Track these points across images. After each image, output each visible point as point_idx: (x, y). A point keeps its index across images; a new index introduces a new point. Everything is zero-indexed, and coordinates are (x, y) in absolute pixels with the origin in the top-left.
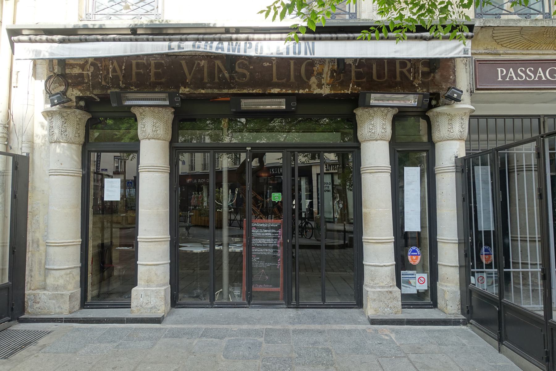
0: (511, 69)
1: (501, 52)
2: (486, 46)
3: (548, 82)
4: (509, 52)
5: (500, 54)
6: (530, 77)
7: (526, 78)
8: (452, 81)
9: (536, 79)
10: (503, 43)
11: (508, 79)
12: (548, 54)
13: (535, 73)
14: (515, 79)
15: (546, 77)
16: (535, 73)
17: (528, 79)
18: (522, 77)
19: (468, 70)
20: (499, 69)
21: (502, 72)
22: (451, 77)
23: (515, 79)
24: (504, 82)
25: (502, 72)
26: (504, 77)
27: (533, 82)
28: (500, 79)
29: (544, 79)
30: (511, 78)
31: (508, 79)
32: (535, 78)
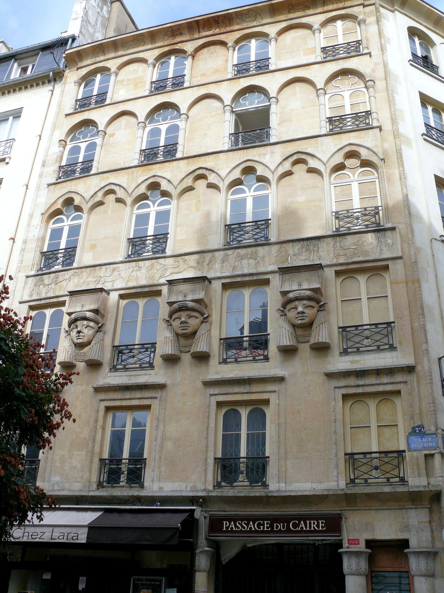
0: (232, 522)
1: (227, 510)
3: (256, 531)
6: (244, 528)
9: (248, 529)
11: (229, 529)
13: (247, 525)
14: (234, 529)
15: (254, 528)
16: (247, 525)
20: (225, 522)
21: (226, 524)
24: (227, 531)
25: (226, 524)
26: (227, 528)
27: (246, 532)
28: (224, 529)
29: (253, 529)
30: (232, 528)
31: (229, 529)
32: (247, 528)
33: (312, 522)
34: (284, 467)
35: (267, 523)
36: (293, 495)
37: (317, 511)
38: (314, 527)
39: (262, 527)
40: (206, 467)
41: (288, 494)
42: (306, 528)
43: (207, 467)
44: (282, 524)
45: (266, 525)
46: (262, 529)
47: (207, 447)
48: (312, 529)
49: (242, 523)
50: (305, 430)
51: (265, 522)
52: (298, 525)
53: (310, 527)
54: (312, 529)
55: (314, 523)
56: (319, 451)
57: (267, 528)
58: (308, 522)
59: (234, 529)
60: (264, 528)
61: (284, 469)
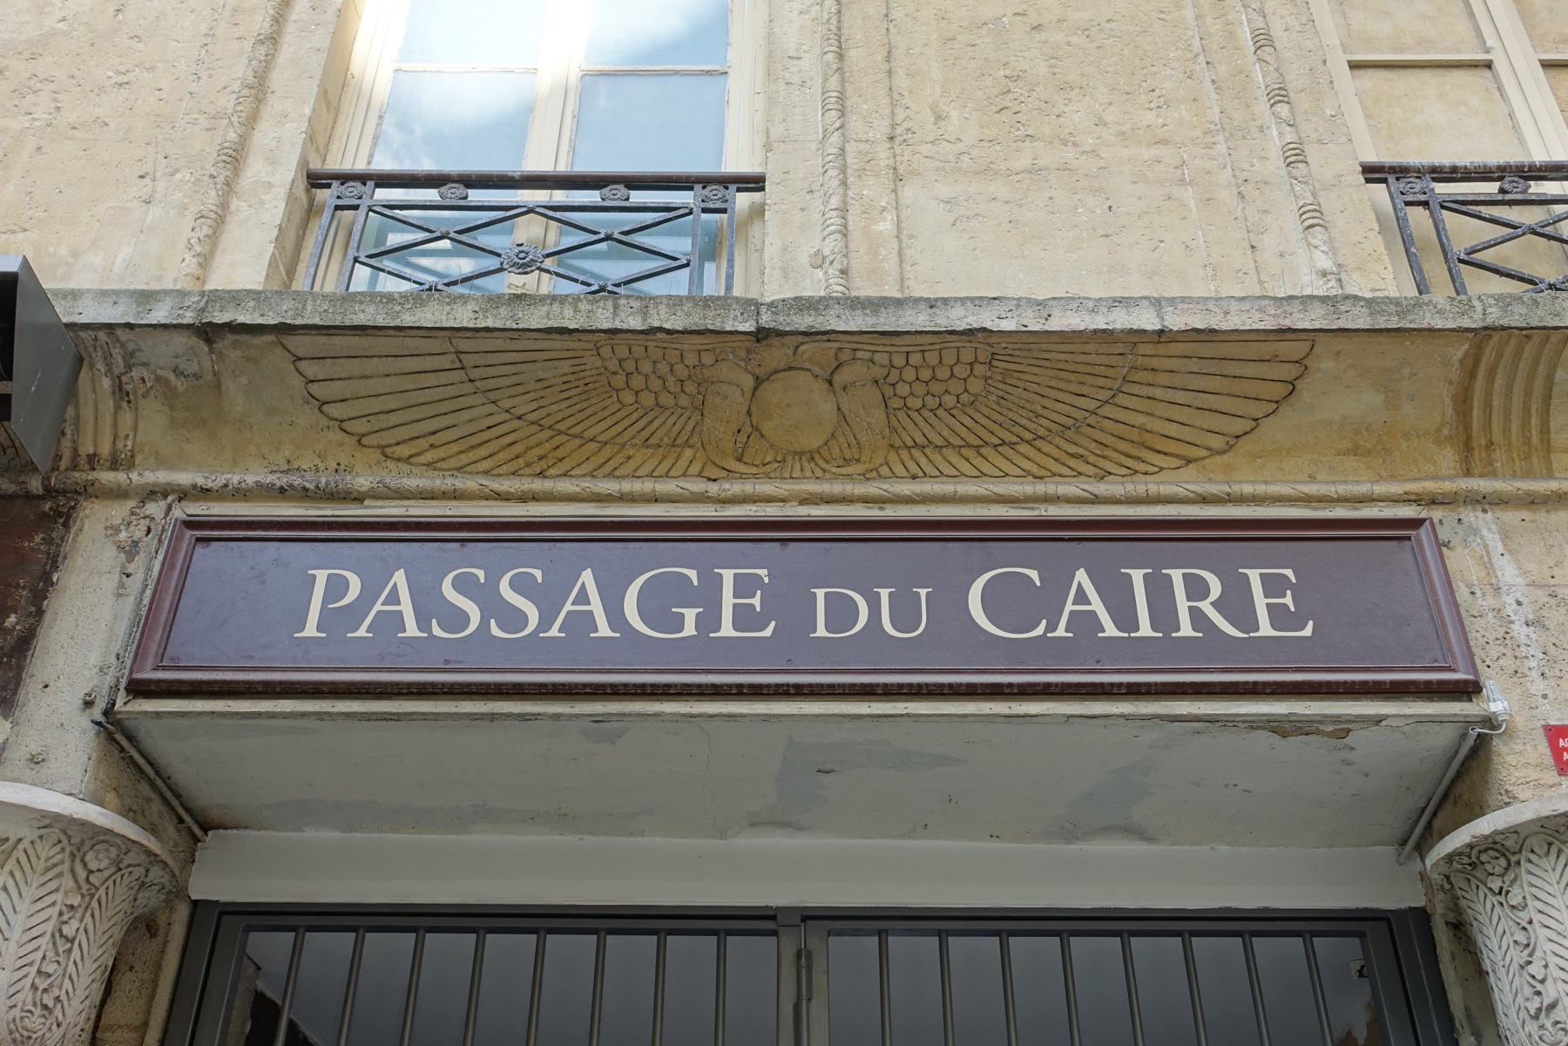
1: (363, 482)
2: (287, 452)
4: (412, 483)
5: (359, 499)
7: (484, 623)
8: (11, 640)
9: (554, 632)
10: (388, 437)
11: (362, 632)
12: (656, 499)
17: (496, 631)
18: (464, 619)
19: (135, 583)
21: (337, 587)
22: (13, 619)
23: (412, 630)
25: (337, 587)
29: (604, 630)
31: (362, 632)
32: (545, 623)
33: (1177, 575)
34: (890, 216)
35: (743, 587)
36: (1009, 325)
37: (1204, 500)
38: (1197, 617)
39: (690, 615)
40: (224, 205)
41: (961, 319)
42: (1126, 619)
43: (235, 204)
44: (884, 593)
45: (728, 600)
46: (690, 629)
47: (259, 88)
48: (1186, 630)
49: (493, 581)
50: (1037, 28)
51: (728, 576)
52: (1049, 601)
53: (1163, 614)
54: (1186, 630)
55: (1197, 589)
56: (1164, 142)
57: (743, 617)
58: (1137, 576)
59: (412, 630)
60: (710, 620)
61: (885, 226)
